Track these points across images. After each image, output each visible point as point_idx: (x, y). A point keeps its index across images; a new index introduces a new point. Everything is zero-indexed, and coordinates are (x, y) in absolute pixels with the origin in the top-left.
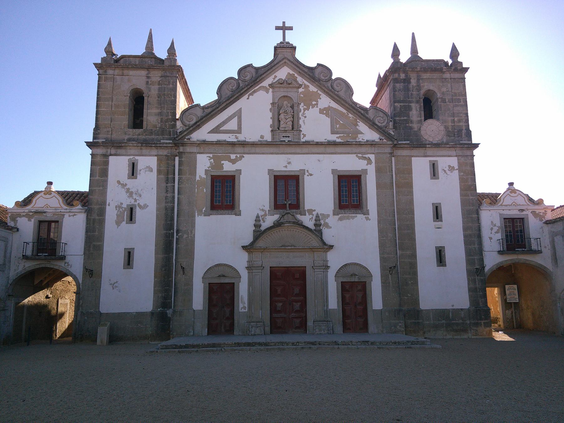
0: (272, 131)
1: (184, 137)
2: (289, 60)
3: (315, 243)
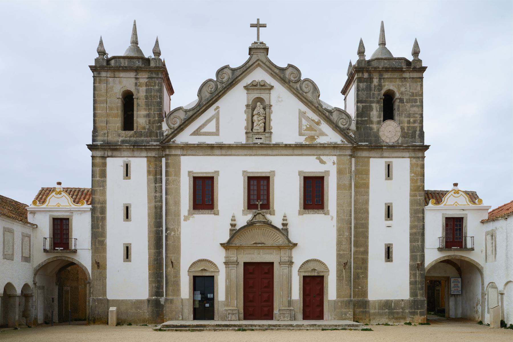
0: (246, 133)
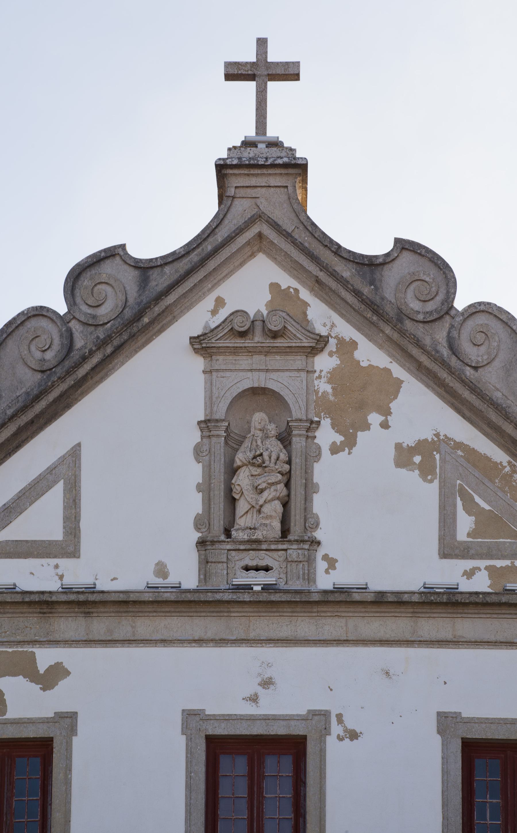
0: (201, 543)
2: (275, 226)
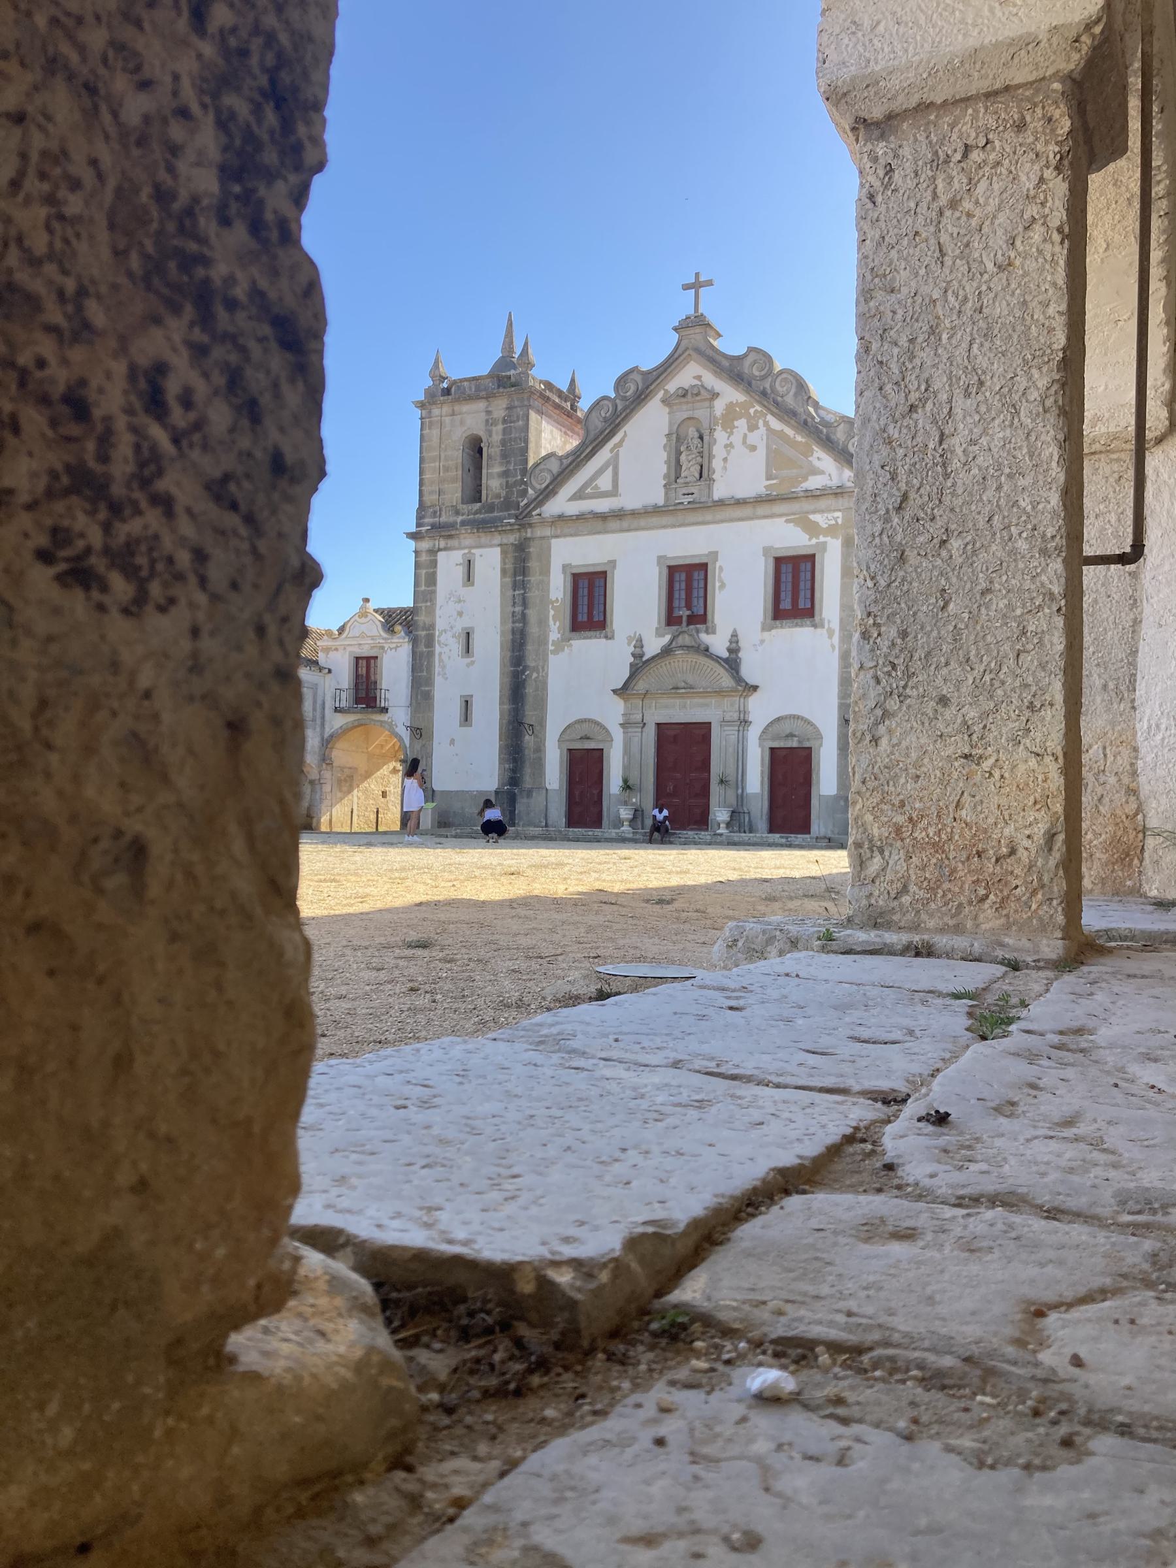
1: (529, 514)
3: (727, 681)
